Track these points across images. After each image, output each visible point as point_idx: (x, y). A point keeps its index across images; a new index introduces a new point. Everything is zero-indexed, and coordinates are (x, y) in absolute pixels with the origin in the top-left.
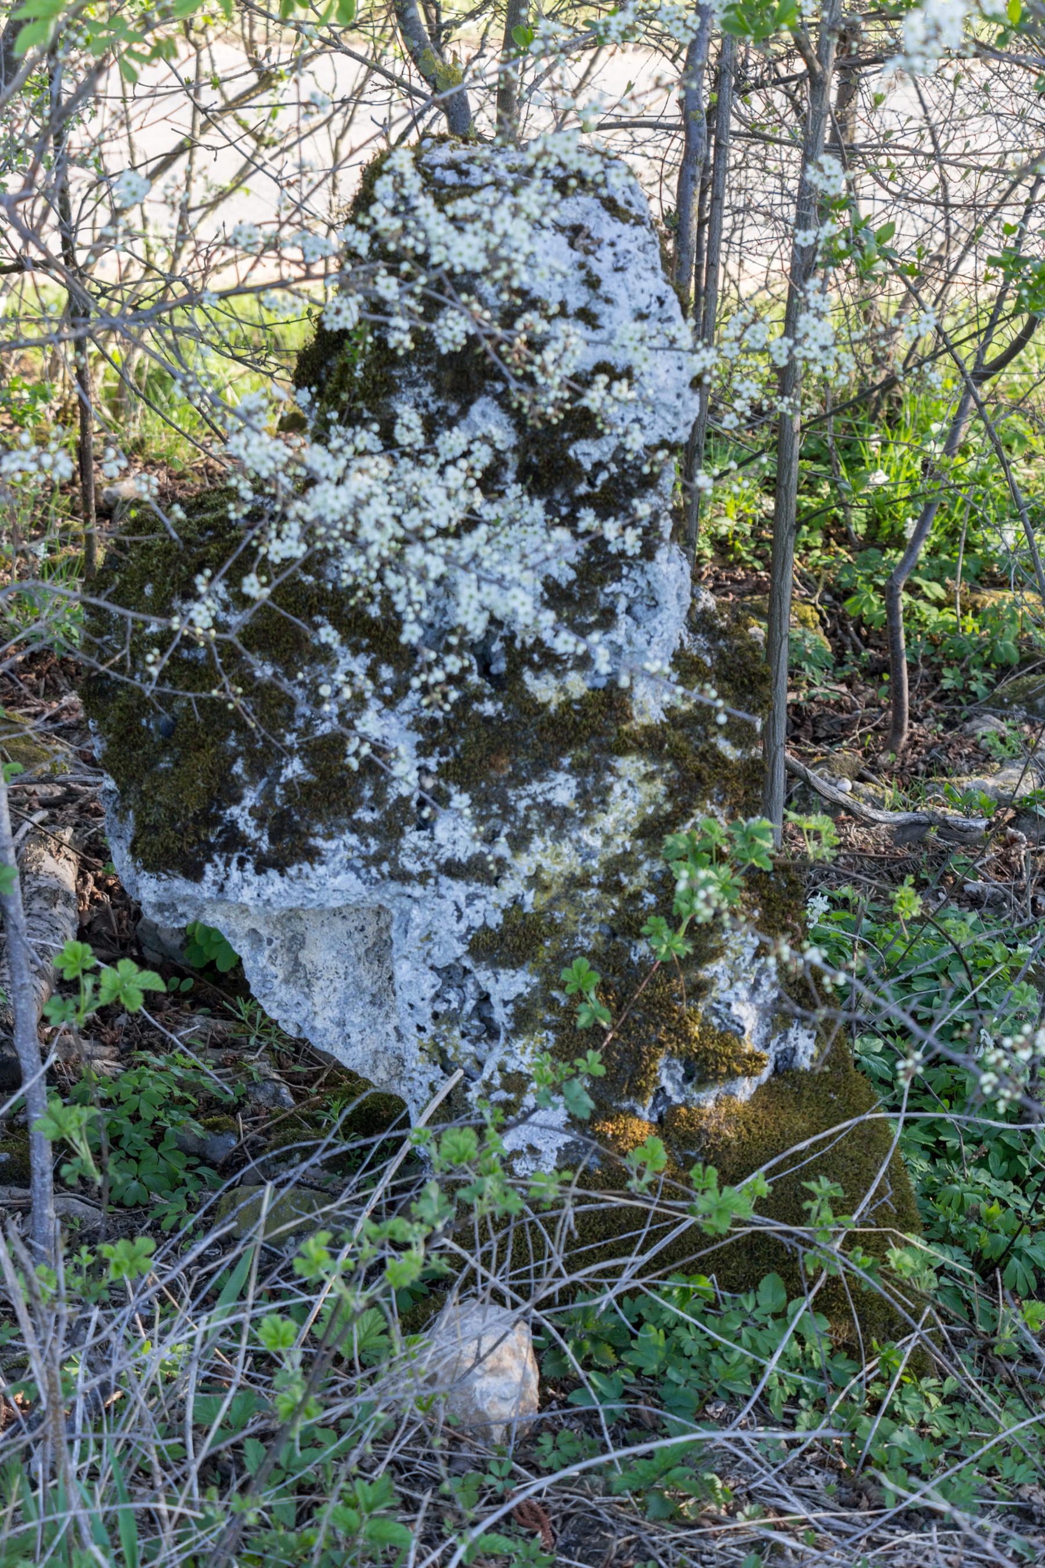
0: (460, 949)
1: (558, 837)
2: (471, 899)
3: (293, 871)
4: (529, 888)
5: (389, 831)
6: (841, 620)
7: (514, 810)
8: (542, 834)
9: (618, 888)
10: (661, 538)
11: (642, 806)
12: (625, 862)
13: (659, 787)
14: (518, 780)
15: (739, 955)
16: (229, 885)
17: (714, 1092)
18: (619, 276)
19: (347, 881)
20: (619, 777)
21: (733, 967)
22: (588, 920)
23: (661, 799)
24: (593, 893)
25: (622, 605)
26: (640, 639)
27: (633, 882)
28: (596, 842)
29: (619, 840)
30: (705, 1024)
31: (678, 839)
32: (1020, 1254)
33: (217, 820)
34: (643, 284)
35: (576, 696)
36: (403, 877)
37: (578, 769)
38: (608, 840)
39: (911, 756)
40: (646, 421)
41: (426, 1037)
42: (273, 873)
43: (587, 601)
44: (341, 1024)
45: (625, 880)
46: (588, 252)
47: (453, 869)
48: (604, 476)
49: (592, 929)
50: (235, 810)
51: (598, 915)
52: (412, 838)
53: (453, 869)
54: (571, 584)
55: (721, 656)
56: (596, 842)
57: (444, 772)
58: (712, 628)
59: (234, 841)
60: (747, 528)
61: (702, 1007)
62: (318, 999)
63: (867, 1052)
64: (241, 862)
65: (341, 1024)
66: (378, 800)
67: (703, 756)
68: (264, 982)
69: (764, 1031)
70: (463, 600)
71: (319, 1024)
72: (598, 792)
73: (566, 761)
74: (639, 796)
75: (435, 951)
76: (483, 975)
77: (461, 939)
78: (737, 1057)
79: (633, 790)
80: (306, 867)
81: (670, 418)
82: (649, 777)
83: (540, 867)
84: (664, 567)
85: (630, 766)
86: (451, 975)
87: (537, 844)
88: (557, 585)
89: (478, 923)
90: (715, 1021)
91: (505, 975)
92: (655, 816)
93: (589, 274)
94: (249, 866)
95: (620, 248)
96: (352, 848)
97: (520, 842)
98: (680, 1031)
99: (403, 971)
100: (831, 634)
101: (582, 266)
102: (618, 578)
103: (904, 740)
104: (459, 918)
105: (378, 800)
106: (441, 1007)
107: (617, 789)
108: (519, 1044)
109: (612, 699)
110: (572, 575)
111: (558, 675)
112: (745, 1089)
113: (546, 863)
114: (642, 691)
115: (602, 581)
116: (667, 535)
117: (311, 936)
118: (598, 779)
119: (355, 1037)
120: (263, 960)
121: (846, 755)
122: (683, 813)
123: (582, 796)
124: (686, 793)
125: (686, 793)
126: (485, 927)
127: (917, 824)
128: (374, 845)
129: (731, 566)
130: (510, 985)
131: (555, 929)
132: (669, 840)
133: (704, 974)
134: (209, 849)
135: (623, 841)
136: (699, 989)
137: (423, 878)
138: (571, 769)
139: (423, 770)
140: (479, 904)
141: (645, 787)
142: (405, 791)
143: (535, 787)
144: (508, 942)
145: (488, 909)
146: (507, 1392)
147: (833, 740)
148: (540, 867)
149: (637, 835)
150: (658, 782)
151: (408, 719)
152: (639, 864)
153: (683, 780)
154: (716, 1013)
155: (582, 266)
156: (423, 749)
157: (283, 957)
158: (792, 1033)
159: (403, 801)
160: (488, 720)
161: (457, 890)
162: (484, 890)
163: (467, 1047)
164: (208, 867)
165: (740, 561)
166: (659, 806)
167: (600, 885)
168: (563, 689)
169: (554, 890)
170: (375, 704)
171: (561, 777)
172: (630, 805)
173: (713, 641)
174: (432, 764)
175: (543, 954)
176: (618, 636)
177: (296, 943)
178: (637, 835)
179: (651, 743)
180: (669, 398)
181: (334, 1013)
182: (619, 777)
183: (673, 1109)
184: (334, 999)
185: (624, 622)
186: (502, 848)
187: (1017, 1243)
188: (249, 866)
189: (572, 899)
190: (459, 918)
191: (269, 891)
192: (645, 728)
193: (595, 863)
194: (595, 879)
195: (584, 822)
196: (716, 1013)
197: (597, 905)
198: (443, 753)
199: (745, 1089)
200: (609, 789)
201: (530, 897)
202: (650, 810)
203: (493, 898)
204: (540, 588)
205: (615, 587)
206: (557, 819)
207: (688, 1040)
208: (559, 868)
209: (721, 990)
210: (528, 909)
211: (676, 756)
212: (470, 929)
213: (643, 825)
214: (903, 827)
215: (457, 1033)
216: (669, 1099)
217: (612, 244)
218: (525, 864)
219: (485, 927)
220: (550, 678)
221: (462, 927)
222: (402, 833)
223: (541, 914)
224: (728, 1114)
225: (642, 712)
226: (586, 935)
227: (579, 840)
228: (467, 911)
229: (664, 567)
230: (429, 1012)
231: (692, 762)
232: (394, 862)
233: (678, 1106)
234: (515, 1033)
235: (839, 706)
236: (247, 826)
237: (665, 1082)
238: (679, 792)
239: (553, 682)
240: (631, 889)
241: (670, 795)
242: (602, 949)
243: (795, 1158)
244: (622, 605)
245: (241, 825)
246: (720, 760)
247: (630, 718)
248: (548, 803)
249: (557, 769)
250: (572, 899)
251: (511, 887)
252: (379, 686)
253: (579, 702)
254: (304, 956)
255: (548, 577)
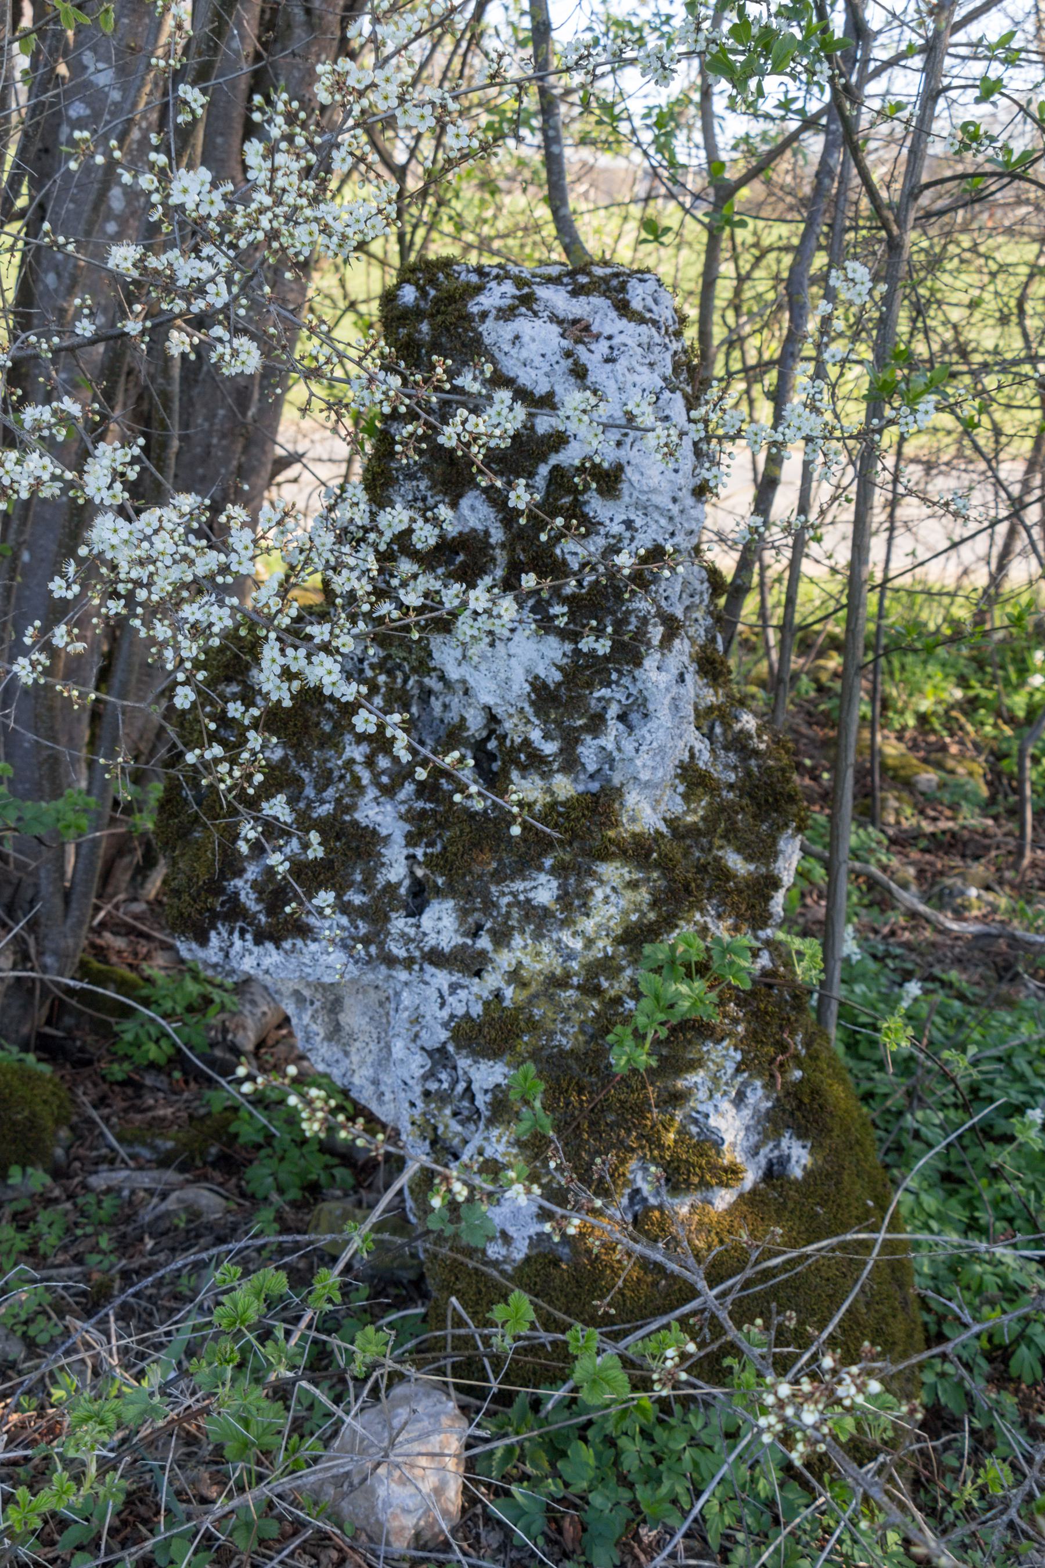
0: (444, 1035)
1: (538, 936)
2: (454, 988)
3: (287, 945)
4: (509, 983)
5: (376, 915)
6: (998, 774)
7: (495, 905)
8: (523, 932)
9: (596, 991)
10: (648, 644)
11: (625, 913)
12: (606, 966)
13: (644, 895)
14: (499, 877)
15: (720, 1067)
16: (233, 952)
17: (688, 1201)
18: (609, 366)
19: (337, 958)
20: (602, 882)
21: (715, 1079)
22: (566, 1020)
23: (645, 908)
24: (570, 995)
25: (613, 710)
26: (628, 746)
27: (612, 987)
28: (578, 944)
29: (600, 944)
30: (682, 1131)
31: (656, 951)
32: (1030, 1342)
33: (222, 891)
34: (636, 378)
35: (562, 798)
36: (391, 961)
37: (560, 870)
38: (589, 943)
39: (1030, 875)
40: (638, 523)
41: (416, 1113)
42: (270, 946)
43: (575, 704)
44: (376, 1082)
45: (605, 984)
46: (579, 341)
47: (436, 958)
48: (589, 579)
49: (572, 1029)
50: (239, 883)
51: (577, 1016)
52: (399, 923)
53: (436, 958)
54: (559, 685)
55: (749, 774)
56: (578, 944)
57: (430, 862)
58: (744, 747)
59: (235, 912)
60: (940, 709)
61: (679, 1115)
62: (355, 1058)
63: (926, 1123)
64: (243, 932)
65: (376, 1082)
66: (367, 885)
67: (702, 869)
68: (308, 1039)
69: (754, 1138)
70: (265, 664)
71: (356, 1080)
72: (578, 896)
73: (548, 862)
74: (623, 903)
75: (423, 1034)
76: (463, 1063)
77: (445, 1025)
78: (713, 1168)
79: (615, 897)
80: (299, 943)
81: (663, 522)
82: (633, 885)
83: (520, 963)
84: (654, 675)
85: (613, 872)
86: (439, 1056)
87: (517, 941)
88: (545, 686)
89: (460, 1011)
90: (694, 1129)
91: (485, 1065)
92: (639, 924)
93: (576, 363)
94: (249, 936)
95: (614, 342)
96: (343, 928)
97: (502, 938)
98: (652, 1140)
99: (398, 1048)
100: (989, 784)
101: (568, 354)
102: (608, 684)
103: (1026, 862)
104: (442, 1005)
105: (367, 885)
106: (433, 1086)
107: (599, 894)
108: (495, 1132)
109: (601, 804)
110: (558, 676)
111: (545, 776)
112: (723, 1199)
113: (526, 960)
114: (632, 798)
115: (590, 685)
116: (656, 642)
117: (348, 1002)
118: (580, 882)
119: (388, 1096)
120: (306, 1019)
121: (978, 869)
122: (669, 922)
123: (563, 898)
124: (673, 901)
125: (673, 901)
126: (467, 1014)
127: (988, 935)
128: (363, 928)
129: (925, 733)
130: (487, 1075)
131: (533, 1025)
132: (647, 949)
133: (680, 1084)
134: (214, 917)
135: (604, 946)
136: (677, 1098)
137: (408, 963)
138: (553, 871)
139: (411, 857)
140: (462, 994)
141: (629, 894)
142: (393, 878)
143: (518, 886)
144: (489, 1032)
145: (470, 998)
146: (411, 1504)
147: (977, 858)
148: (520, 963)
149: (619, 941)
150: (643, 890)
151: (403, 809)
152: (621, 969)
153: (671, 891)
154: (696, 1122)
155: (568, 354)
156: (411, 840)
157: (323, 1017)
158: (785, 1143)
159: (391, 888)
160: (472, 815)
161: (441, 978)
162: (465, 981)
163: (456, 1127)
164: (213, 934)
165: (934, 731)
166: (644, 915)
167: (579, 987)
168: (549, 791)
169: (534, 987)
170: (372, 792)
171: (543, 878)
172: (613, 910)
173: (744, 760)
174: (419, 852)
175: (520, 1048)
176: (608, 742)
177: (335, 1006)
178: (619, 941)
179: (639, 851)
180: (663, 500)
181: (368, 1072)
182: (602, 882)
183: (649, 1209)
184: (369, 1059)
185: (614, 727)
186: (484, 942)
187: (1029, 1331)
188: (249, 936)
189: (551, 998)
190: (442, 1005)
191: (267, 962)
192: (634, 835)
193: (575, 965)
194: (575, 980)
195: (565, 923)
196: (696, 1122)
197: (577, 1006)
198: (431, 844)
199: (723, 1199)
200: (590, 893)
201: (509, 992)
202: (634, 917)
203: (475, 989)
204: (527, 688)
205: (604, 692)
206: (538, 919)
207: (661, 1147)
208: (539, 967)
209: (700, 1100)
210: (507, 1003)
211: (666, 865)
212: (452, 1016)
213: (626, 931)
214: (977, 937)
215: (448, 1112)
216: (645, 1200)
217: (610, 338)
218: (505, 959)
219: (467, 1014)
220: (536, 778)
221: (445, 1014)
222: (387, 919)
223: (519, 1009)
224: (700, 1223)
225: (633, 820)
226: (564, 1034)
227: (559, 941)
228: (450, 1000)
229: (654, 675)
230: (418, 1090)
231: (684, 871)
232: (381, 945)
233: (653, 1208)
234: (491, 1122)
235: (985, 834)
236: (249, 900)
237: (640, 1183)
238: (665, 902)
239: (539, 783)
240: (612, 993)
241: (654, 904)
242: (582, 1048)
243: (767, 1274)
244: (613, 710)
245: (243, 897)
246: (725, 874)
247: (616, 824)
248: (528, 901)
249: (540, 868)
250: (551, 998)
251: (493, 980)
252: (376, 776)
253: (563, 804)
254: (343, 1018)
255: (537, 677)
